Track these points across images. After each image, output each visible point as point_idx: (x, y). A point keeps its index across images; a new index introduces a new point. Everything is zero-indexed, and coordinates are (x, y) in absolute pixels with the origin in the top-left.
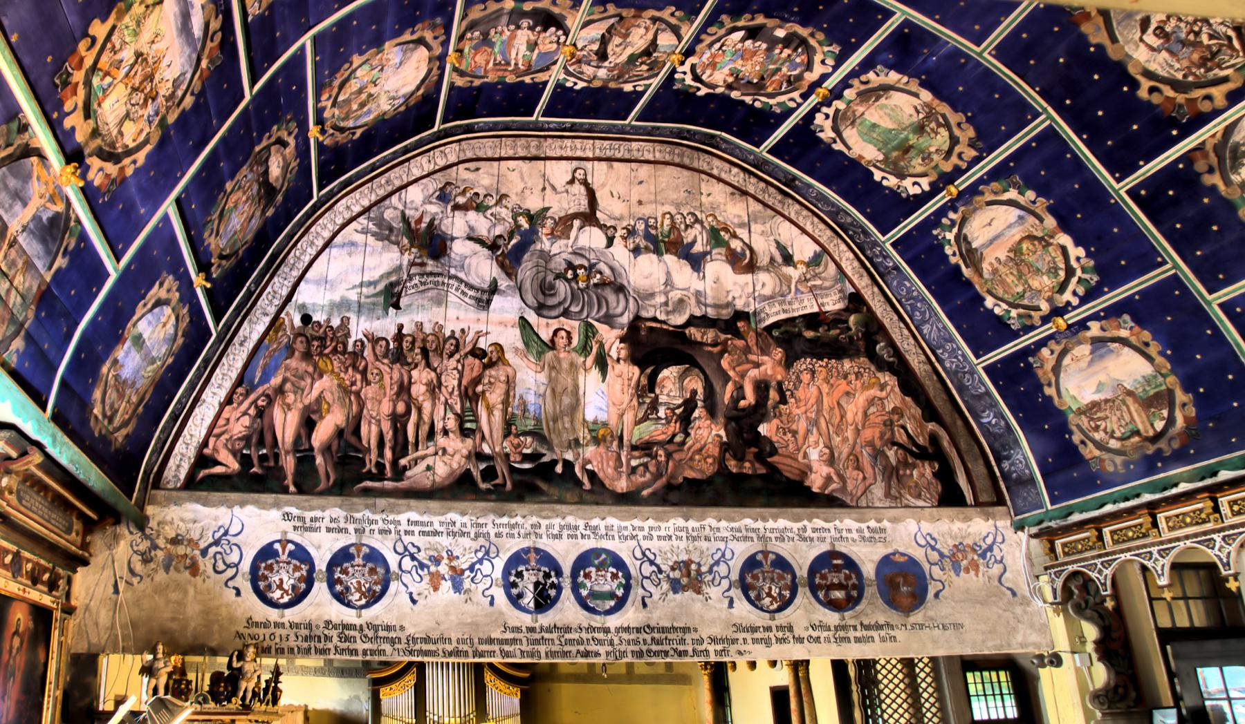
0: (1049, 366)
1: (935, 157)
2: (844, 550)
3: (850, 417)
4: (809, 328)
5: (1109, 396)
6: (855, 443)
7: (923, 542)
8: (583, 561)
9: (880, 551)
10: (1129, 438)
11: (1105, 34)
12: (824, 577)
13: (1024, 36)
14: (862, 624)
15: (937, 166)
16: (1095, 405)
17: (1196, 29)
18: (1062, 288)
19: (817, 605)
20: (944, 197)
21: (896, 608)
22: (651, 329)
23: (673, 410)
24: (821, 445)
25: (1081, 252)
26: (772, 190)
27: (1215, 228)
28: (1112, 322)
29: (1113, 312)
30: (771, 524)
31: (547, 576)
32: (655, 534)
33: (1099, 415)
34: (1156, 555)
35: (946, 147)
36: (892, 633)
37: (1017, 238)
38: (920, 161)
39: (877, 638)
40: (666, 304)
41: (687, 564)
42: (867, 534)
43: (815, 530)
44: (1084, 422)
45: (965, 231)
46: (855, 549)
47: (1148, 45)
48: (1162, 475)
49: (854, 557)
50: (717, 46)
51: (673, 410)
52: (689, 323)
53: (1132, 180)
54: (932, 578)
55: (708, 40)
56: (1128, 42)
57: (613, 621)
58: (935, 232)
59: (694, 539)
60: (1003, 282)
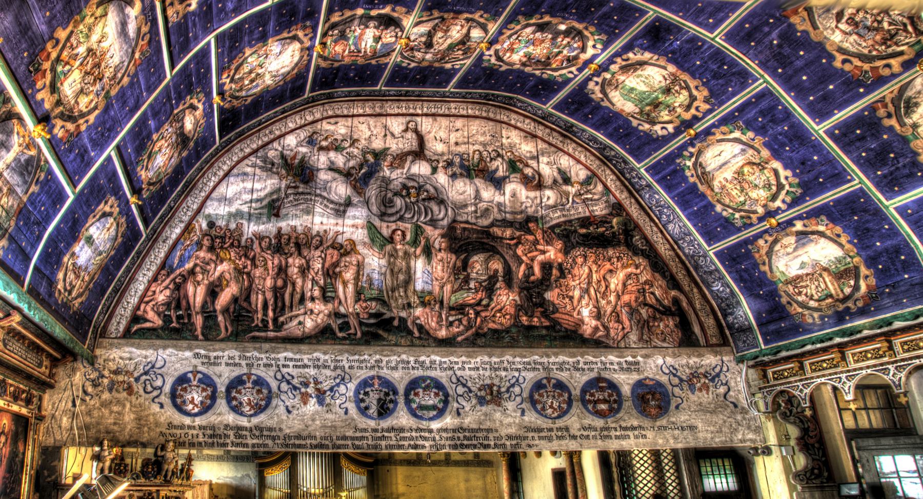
0: (763, 252)
1: (679, 110)
2: (607, 376)
3: (612, 286)
4: (582, 226)
6: (616, 306)
7: (667, 371)
8: (413, 385)
9: (635, 377)
10: (824, 299)
11: (809, 23)
12: (592, 395)
13: (747, 26)
14: (620, 426)
15: (679, 116)
16: (799, 277)
17: (879, 18)
18: (774, 198)
19: (587, 414)
20: (685, 137)
21: (646, 416)
22: (464, 229)
23: (480, 283)
24: (591, 306)
25: (789, 173)
26: (555, 134)
27: (892, 155)
29: (815, 214)
30: (552, 360)
31: (387, 394)
32: (467, 366)
33: (801, 284)
34: (844, 379)
35: (686, 103)
36: (644, 433)
37: (741, 164)
38: (667, 112)
39: (632, 436)
40: (476, 212)
41: (491, 386)
42: (625, 366)
43: (585, 363)
44: (790, 289)
45: (700, 160)
46: (616, 376)
47: (841, 31)
48: (849, 325)
49: (615, 381)
50: (515, 37)
51: (480, 283)
52: (492, 225)
53: (828, 123)
54: (673, 395)
55: (509, 33)
56: (827, 29)
57: (435, 425)
58: (678, 161)
59: (496, 370)
60: (729, 194)
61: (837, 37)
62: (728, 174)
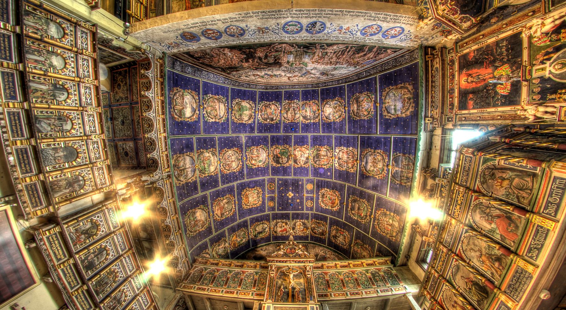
0: (194, 95)
16: (183, 99)
18: (206, 112)
25: (211, 121)
28: (197, 117)
29: (199, 118)
61: (230, 152)
62: (217, 107)
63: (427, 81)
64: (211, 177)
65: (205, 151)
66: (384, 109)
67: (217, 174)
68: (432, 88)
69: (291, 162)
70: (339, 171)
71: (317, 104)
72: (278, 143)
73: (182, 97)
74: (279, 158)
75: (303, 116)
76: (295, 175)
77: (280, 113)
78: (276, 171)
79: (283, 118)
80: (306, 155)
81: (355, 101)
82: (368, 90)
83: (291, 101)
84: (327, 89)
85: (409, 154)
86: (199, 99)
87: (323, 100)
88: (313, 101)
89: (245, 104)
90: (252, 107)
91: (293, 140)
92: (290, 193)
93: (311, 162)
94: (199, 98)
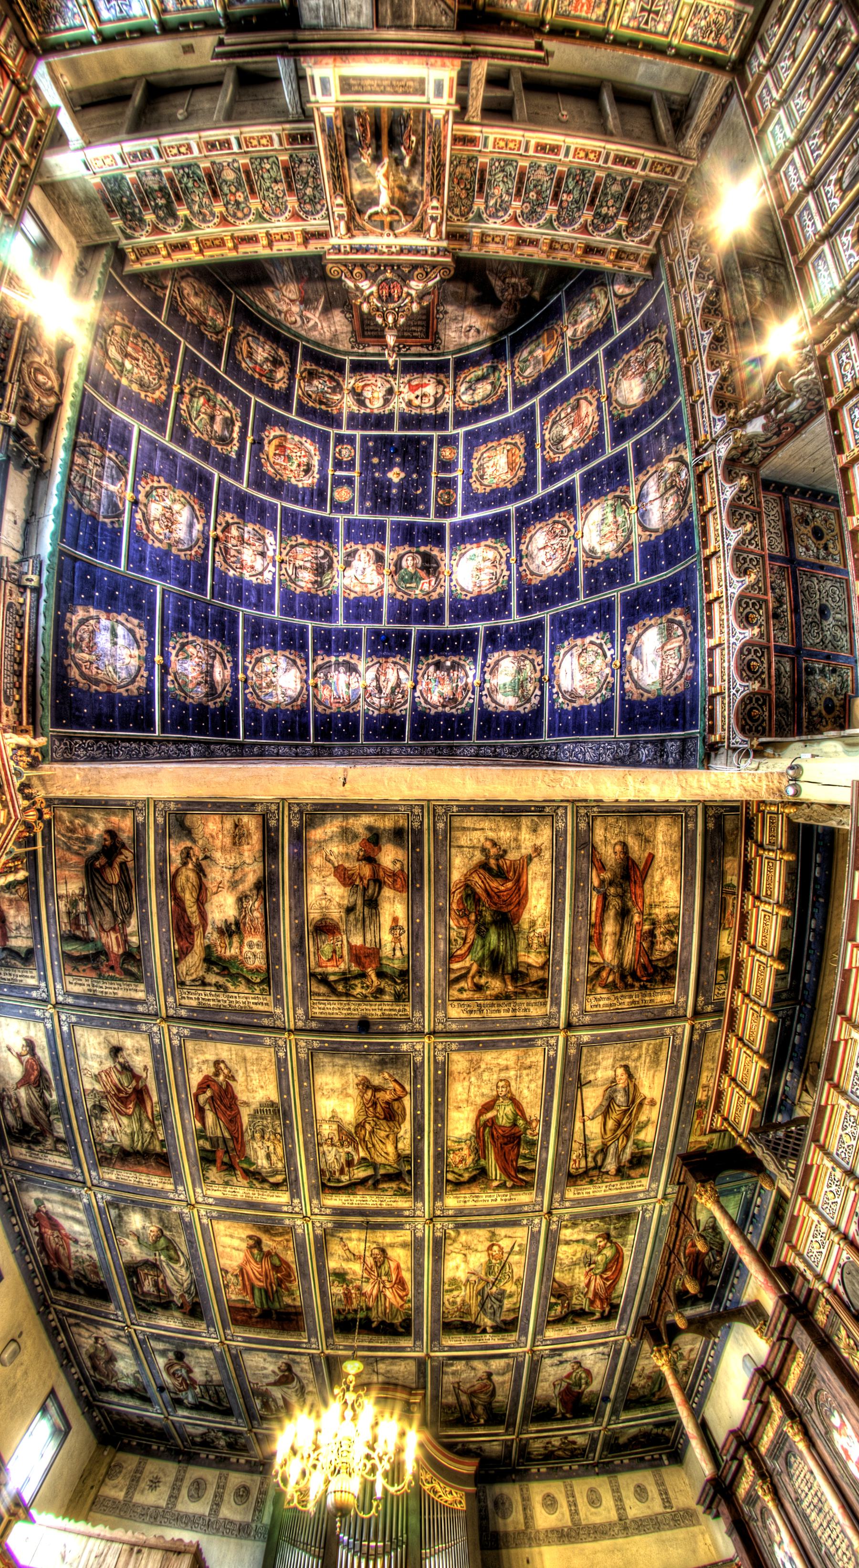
0: (634, 690)
5: (659, 661)
18: (605, 656)
62: (578, 676)
63: (32, 677)
64: (599, 494)
65: (612, 555)
66: (144, 645)
67: (584, 504)
68: (22, 659)
69: (390, 556)
70: (262, 524)
71: (320, 702)
72: (422, 603)
73: (663, 678)
74: (422, 568)
75: (357, 671)
76: (382, 526)
77: (416, 682)
78: (434, 535)
79: (410, 667)
80: (349, 572)
81: (220, 689)
82: (184, 706)
83: (387, 714)
84: (292, 737)
85: (80, 512)
86: (622, 683)
87: (303, 712)
88: (328, 712)
89: (508, 701)
90: (490, 694)
91: (385, 610)
92: (396, 480)
93: (339, 557)
94: (622, 688)
